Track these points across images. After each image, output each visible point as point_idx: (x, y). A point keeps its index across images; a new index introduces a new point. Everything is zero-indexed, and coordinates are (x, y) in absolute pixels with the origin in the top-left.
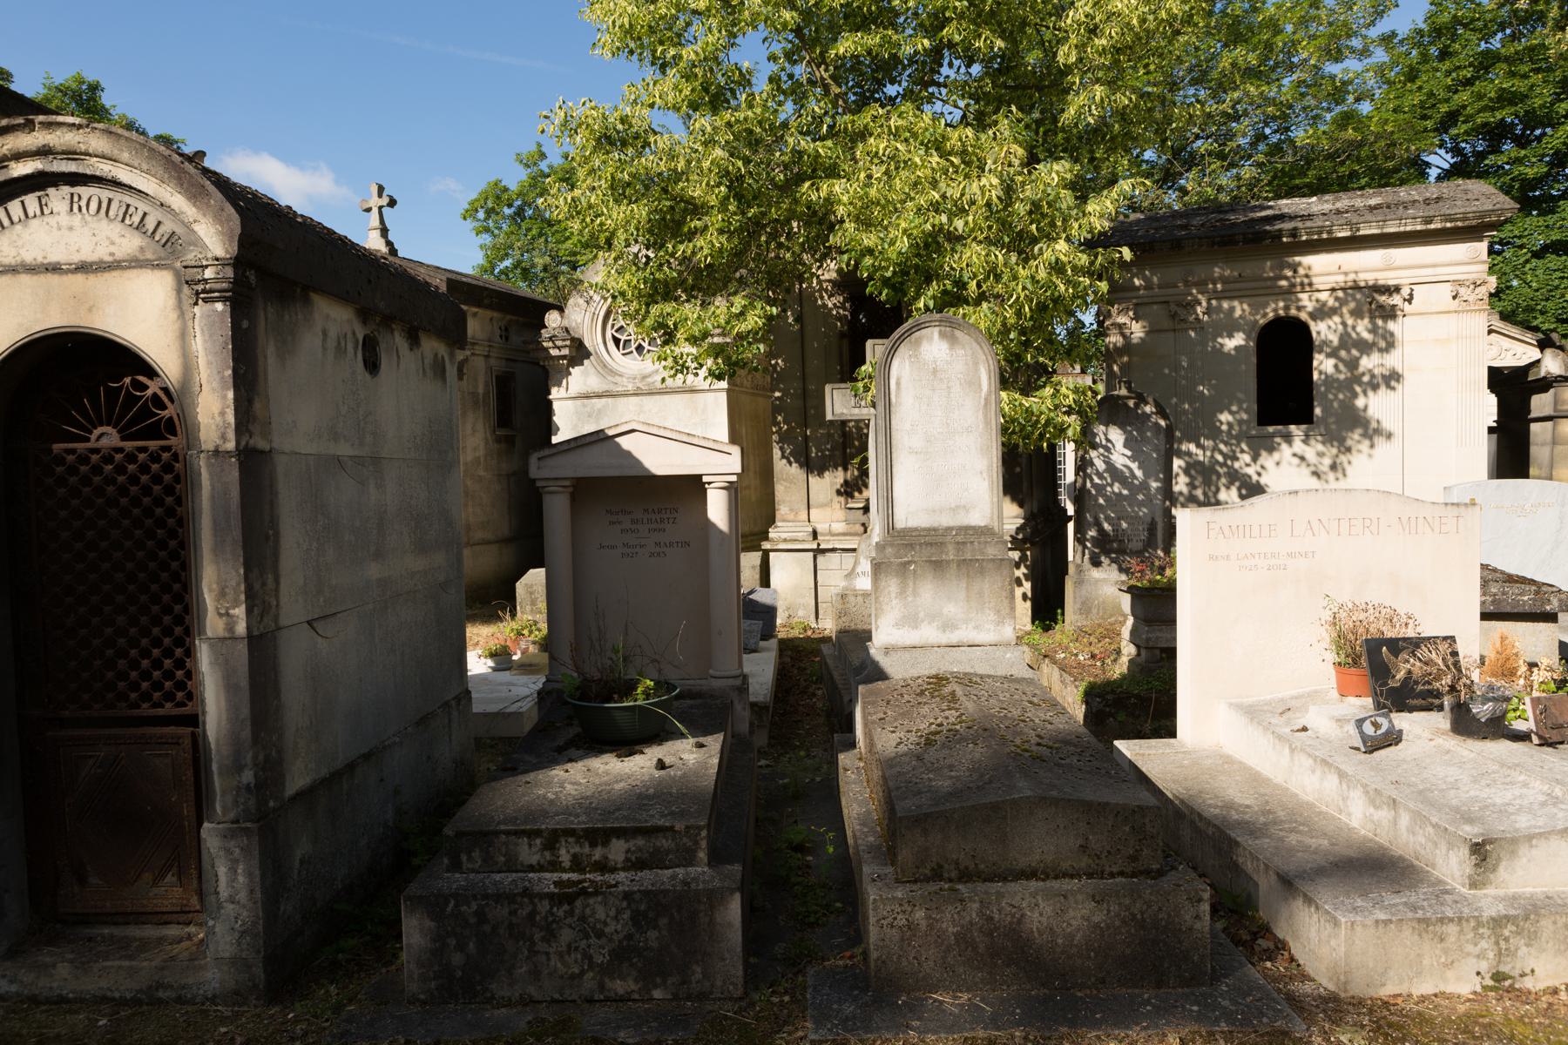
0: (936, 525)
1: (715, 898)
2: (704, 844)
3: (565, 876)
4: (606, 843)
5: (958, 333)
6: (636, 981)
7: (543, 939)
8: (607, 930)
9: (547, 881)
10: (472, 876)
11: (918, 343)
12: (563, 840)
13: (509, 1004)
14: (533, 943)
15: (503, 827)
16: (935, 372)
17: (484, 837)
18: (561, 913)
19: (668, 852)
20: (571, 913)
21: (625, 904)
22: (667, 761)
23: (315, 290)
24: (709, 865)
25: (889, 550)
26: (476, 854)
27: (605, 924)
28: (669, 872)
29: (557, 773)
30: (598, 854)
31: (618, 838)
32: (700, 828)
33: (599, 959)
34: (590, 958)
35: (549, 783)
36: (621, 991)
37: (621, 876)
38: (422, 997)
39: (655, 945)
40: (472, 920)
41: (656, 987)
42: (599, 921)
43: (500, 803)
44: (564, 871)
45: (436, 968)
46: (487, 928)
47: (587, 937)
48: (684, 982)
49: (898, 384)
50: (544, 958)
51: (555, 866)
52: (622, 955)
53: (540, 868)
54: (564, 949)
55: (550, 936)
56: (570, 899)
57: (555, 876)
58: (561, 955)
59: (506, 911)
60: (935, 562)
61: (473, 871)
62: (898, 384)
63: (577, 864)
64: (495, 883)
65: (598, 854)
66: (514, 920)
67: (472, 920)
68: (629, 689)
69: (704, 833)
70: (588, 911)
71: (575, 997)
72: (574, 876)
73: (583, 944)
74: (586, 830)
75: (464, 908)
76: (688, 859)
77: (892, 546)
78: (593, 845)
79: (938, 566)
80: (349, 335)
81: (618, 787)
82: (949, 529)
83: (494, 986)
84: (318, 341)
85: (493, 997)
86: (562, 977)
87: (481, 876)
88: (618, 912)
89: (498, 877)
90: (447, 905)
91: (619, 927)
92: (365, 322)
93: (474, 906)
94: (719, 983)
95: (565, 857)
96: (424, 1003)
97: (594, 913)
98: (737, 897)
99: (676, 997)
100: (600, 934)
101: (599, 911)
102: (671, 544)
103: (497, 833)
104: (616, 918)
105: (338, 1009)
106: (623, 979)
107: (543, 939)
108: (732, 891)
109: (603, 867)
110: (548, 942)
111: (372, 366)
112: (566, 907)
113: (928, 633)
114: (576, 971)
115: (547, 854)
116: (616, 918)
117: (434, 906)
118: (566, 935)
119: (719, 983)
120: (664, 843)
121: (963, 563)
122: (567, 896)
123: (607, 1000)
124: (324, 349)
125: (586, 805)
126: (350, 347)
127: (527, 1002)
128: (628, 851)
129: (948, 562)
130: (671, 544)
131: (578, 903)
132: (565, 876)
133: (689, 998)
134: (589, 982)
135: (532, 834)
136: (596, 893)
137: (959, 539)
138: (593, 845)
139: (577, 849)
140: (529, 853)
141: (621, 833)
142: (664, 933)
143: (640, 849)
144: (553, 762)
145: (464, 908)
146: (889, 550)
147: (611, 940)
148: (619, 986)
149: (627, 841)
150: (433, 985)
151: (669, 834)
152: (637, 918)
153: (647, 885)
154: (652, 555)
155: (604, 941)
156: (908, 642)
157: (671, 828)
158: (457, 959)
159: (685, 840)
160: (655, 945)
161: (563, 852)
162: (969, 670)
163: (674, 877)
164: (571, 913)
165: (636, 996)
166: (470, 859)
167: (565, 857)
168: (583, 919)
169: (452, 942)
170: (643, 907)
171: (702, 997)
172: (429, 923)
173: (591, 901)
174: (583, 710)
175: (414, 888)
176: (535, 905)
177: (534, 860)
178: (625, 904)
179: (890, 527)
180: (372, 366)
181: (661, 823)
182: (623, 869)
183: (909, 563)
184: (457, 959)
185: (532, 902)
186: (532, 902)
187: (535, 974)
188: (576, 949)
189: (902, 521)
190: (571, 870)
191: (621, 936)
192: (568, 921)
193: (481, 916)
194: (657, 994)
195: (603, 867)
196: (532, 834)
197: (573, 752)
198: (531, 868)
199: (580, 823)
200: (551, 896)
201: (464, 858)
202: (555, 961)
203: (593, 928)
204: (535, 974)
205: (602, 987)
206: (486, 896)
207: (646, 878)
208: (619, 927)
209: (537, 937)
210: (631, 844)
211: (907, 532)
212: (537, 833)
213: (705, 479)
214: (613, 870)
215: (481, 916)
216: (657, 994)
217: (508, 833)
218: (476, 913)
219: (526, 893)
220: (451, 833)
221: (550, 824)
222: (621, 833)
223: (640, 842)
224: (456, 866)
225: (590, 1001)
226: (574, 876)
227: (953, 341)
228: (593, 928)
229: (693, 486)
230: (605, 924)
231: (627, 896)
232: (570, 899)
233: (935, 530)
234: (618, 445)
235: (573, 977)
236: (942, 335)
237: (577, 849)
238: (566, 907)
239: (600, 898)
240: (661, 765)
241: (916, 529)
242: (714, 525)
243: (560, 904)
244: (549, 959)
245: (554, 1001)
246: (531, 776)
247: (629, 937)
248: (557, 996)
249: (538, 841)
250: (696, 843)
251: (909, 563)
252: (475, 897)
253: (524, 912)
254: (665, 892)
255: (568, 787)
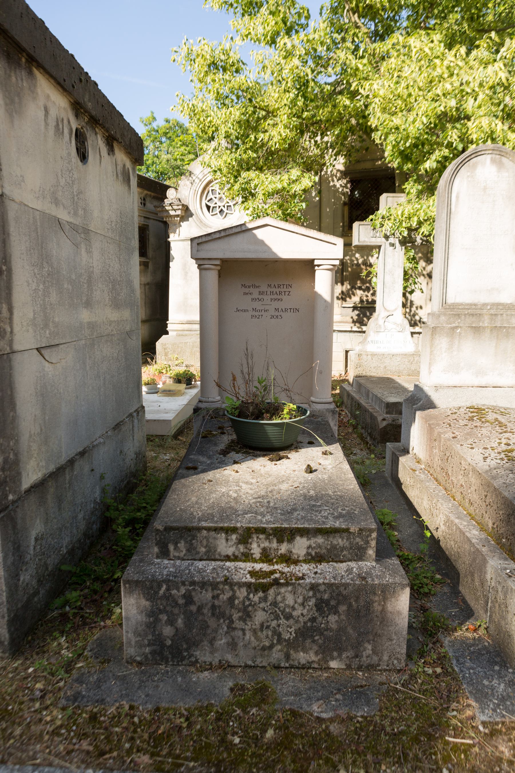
0: (476, 301)
1: (387, 592)
2: (373, 543)
3: (258, 566)
4: (291, 540)
5: (504, 160)
6: (316, 653)
7: (240, 619)
8: (295, 613)
9: (242, 571)
10: (178, 562)
11: (475, 166)
12: (254, 536)
13: (210, 667)
14: (232, 622)
15: (204, 524)
16: (485, 189)
17: (187, 532)
18: (256, 599)
19: (343, 549)
20: (265, 599)
21: (311, 593)
22: (314, 466)
23: (40, 66)
24: (377, 561)
25: (443, 318)
26: (182, 545)
27: (293, 608)
28: (343, 566)
29: (229, 472)
30: (284, 548)
31: (302, 536)
32: (371, 531)
33: (286, 636)
34: (279, 635)
35: (227, 482)
36: (303, 661)
37: (304, 568)
38: (138, 659)
39: (334, 626)
40: (181, 601)
41: (333, 659)
42: (289, 606)
43: (194, 499)
44: (255, 561)
45: (150, 637)
46: (194, 608)
47: (277, 618)
48: (357, 656)
49: (457, 197)
50: (240, 633)
51: (247, 557)
52: (306, 633)
53: (236, 559)
54: (258, 627)
55: (247, 615)
56: (265, 588)
57: (249, 566)
58: (255, 632)
59: (209, 595)
60: (475, 327)
61: (179, 558)
62: (457, 197)
63: (266, 557)
64: (199, 571)
65: (284, 548)
66: (216, 603)
67: (181, 601)
68: (275, 410)
69: (374, 535)
70: (279, 598)
71: (264, 664)
72: (265, 567)
73: (274, 623)
74: (275, 530)
75: (174, 592)
76: (359, 554)
77: (445, 315)
78: (280, 541)
79: (477, 330)
80: (65, 121)
81: (284, 487)
82: (485, 305)
83: (198, 653)
84: (41, 114)
85: (197, 661)
86: (255, 648)
87: (186, 563)
88: (306, 599)
89: (200, 564)
90: (160, 589)
91: (305, 612)
92: (77, 116)
93: (183, 590)
94: (385, 658)
95: (256, 550)
96: (140, 664)
97: (284, 599)
98: (407, 591)
99: (349, 667)
100: (288, 617)
101: (288, 598)
102: (286, 310)
103: (199, 529)
104: (303, 604)
105: (69, 667)
106: (305, 651)
107: (240, 619)
108: (403, 587)
109: (288, 559)
110: (244, 621)
111: (83, 157)
112: (261, 594)
113: (466, 377)
114: (267, 644)
115: (242, 548)
116: (303, 604)
117: (149, 588)
118: (260, 617)
119: (385, 658)
120: (340, 541)
121: (494, 328)
122: (262, 585)
123: (292, 667)
124: (47, 124)
125: (265, 504)
126: (66, 131)
127: (225, 666)
128: (309, 547)
129: (484, 328)
130: (286, 310)
131: (271, 592)
132: (258, 566)
133: (360, 668)
134: (276, 655)
135: (229, 531)
136: (287, 584)
137: (492, 312)
138: (280, 541)
139: (266, 544)
140: (225, 546)
141: (304, 532)
142: (343, 617)
143: (319, 546)
144: (222, 464)
145: (174, 592)
146: (443, 318)
147: (297, 622)
148: (302, 657)
149: (309, 539)
150: (147, 650)
151: (345, 535)
152: (321, 606)
153: (329, 579)
154: (272, 317)
155: (291, 621)
156: (451, 383)
157: (347, 530)
158: (168, 631)
159: (358, 540)
160: (334, 626)
161: (254, 546)
162: (495, 404)
163: (349, 571)
164: (265, 599)
165: (316, 666)
166: (176, 548)
167: (256, 550)
168: (275, 604)
169: (164, 617)
170: (326, 597)
171: (371, 668)
172: (145, 603)
173: (283, 590)
174: (241, 427)
175: (131, 572)
176: (234, 592)
177: (230, 551)
178: (311, 593)
179: (444, 302)
180: (83, 157)
181: (337, 525)
182: (305, 561)
183: (457, 327)
184: (168, 631)
185: (232, 590)
186: (232, 590)
187: (233, 645)
188: (268, 627)
189: (450, 300)
190: (261, 560)
191: (306, 619)
192: (262, 605)
193: (189, 599)
194: (334, 664)
195: (288, 559)
196: (229, 531)
197: (233, 455)
198: (228, 558)
199: (268, 521)
200: (248, 585)
201: (171, 547)
202: (248, 635)
203: (283, 612)
204: (233, 645)
205: (288, 657)
206: (193, 583)
207: (329, 572)
208: (305, 612)
209: (236, 616)
210: (313, 542)
211: (454, 307)
212: (234, 530)
213: (316, 262)
214: (296, 562)
215: (189, 599)
216: (334, 664)
217: (209, 529)
218: (184, 596)
219: (227, 581)
220: (161, 528)
221: (241, 523)
222: (304, 532)
223: (320, 540)
224: (164, 553)
225: (277, 667)
226: (265, 567)
227: (500, 165)
228: (283, 612)
229: (308, 266)
230: (293, 608)
231: (314, 587)
232: (265, 588)
233: (475, 305)
234: (255, 235)
235: (264, 649)
236: (493, 161)
237: (266, 544)
238: (261, 594)
239: (290, 588)
240: (310, 470)
241: (461, 304)
242: (320, 296)
243: (256, 591)
244: (244, 634)
245: (247, 666)
246: (210, 475)
247: (313, 620)
248: (250, 663)
249: (234, 537)
250: (367, 542)
251: (457, 327)
252: (183, 583)
253: (224, 597)
254: (346, 585)
255: (244, 486)
